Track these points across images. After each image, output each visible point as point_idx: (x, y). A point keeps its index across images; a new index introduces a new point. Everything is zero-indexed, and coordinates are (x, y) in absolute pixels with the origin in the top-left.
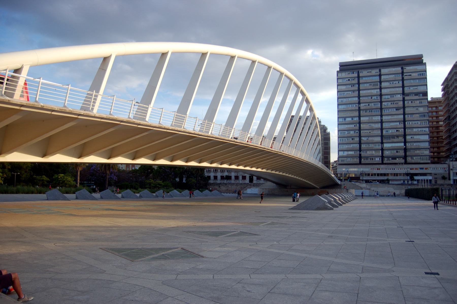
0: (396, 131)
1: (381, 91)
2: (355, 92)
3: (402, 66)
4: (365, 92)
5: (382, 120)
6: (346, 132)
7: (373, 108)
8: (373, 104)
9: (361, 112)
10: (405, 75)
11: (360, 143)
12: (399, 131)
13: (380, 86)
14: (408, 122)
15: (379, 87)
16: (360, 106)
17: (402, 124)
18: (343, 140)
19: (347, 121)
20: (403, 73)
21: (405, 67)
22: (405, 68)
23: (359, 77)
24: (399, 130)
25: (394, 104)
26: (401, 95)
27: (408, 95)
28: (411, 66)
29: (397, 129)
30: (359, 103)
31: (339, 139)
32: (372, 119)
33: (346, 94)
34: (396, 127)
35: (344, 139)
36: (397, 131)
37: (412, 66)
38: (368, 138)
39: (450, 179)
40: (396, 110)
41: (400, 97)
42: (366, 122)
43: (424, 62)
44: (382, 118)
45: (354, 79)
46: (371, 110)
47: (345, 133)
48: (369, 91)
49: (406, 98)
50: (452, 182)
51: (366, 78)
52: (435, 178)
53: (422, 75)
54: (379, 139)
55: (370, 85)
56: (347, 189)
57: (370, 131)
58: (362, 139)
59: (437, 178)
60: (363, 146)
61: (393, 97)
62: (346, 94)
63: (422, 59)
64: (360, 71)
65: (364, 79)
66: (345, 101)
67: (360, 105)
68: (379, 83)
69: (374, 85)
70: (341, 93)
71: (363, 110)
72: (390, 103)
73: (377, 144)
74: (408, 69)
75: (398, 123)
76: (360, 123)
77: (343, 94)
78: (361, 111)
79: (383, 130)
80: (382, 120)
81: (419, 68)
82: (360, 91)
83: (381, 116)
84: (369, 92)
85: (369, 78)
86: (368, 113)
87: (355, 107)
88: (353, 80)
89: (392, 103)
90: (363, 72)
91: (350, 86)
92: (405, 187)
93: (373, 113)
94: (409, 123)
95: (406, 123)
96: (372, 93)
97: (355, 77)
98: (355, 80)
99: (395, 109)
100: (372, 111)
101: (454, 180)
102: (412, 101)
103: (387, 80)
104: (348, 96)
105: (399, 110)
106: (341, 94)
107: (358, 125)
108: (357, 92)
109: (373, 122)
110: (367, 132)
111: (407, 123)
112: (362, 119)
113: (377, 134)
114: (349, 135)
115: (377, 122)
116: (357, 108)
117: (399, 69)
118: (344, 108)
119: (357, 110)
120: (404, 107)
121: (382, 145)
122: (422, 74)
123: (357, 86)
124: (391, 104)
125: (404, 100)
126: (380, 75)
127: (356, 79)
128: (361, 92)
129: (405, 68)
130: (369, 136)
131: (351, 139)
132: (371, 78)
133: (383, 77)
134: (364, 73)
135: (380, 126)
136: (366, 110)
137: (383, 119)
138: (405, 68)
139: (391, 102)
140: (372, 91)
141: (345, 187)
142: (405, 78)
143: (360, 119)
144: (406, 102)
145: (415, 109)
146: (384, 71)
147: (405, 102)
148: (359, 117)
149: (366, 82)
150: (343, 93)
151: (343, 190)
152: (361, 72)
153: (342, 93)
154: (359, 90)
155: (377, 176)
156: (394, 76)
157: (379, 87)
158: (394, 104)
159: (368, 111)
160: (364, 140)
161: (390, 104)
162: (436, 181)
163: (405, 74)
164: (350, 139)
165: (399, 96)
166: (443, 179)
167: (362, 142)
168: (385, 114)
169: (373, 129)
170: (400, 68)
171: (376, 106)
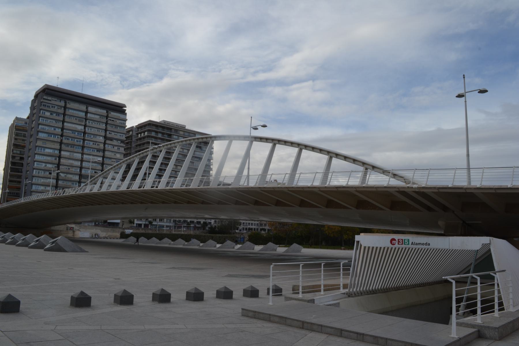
0: (94, 172)
1: (85, 128)
2: (59, 122)
3: (107, 110)
4: (69, 125)
5: (82, 158)
6: (44, 164)
7: (76, 144)
8: (76, 140)
9: (63, 146)
10: (109, 119)
11: (57, 179)
12: (98, 172)
13: (85, 123)
14: (106, 165)
15: (84, 124)
16: (62, 139)
17: (100, 166)
18: (39, 173)
19: (46, 152)
20: (107, 117)
21: (110, 111)
22: (110, 113)
23: (65, 108)
24: (97, 171)
25: (95, 144)
26: (103, 138)
27: (111, 139)
28: (115, 112)
29: (96, 171)
30: (62, 136)
31: (34, 170)
32: (73, 155)
33: (49, 121)
34: (95, 168)
35: (40, 171)
36: (95, 172)
37: (117, 113)
38: (66, 175)
39: (134, 224)
40: (97, 151)
41: (102, 139)
42: (67, 157)
43: (126, 112)
44: (82, 157)
45: (60, 108)
46: (73, 145)
47: (42, 165)
48: (74, 126)
49: (108, 142)
50: (135, 225)
51: (73, 111)
52: (123, 222)
53: (123, 124)
54: (77, 178)
55: (76, 119)
56: (74, 231)
57: (69, 167)
58: (60, 175)
59: (124, 222)
60: (60, 182)
61: (96, 137)
62: (49, 121)
63: (125, 108)
64: (67, 102)
65: (70, 111)
66: (48, 130)
67: (62, 138)
68: (84, 120)
69: (79, 121)
70: (44, 119)
71: (65, 144)
72: (92, 143)
73: (75, 183)
74: (113, 114)
75: (54, 158)
76: (60, 157)
77: (46, 120)
78: (63, 144)
79: (83, 169)
80: (82, 158)
81: (121, 116)
82: (65, 123)
83: (83, 154)
84: (74, 126)
85: (75, 112)
86: (69, 148)
87: (58, 139)
88: (59, 108)
89: (94, 143)
90: (71, 104)
91: (55, 114)
92: (111, 229)
93: (76, 150)
94: (107, 166)
95: (104, 165)
96: (77, 128)
97: (61, 107)
98: (61, 109)
99: (96, 150)
100: (73, 147)
101: (137, 224)
102: (114, 146)
103: (92, 119)
104: (51, 125)
105: (98, 152)
106: (44, 120)
107: (58, 159)
108: (61, 123)
109: (74, 158)
110: (66, 168)
111: (105, 166)
112: (63, 153)
113: (76, 172)
114: (46, 168)
115: (77, 160)
116: (59, 140)
117: (104, 112)
118: (45, 136)
119: (58, 142)
120: (104, 151)
121: (79, 184)
122: (123, 123)
123: (62, 117)
124: (93, 144)
125: (105, 144)
126: (87, 112)
127: (63, 109)
128: (65, 124)
129: (110, 112)
130: (67, 173)
131: (48, 173)
132: (77, 112)
133: (89, 115)
134: (71, 105)
135: (80, 164)
136: (68, 145)
137: (84, 158)
138: (110, 112)
139: (93, 143)
140: (77, 126)
141: (71, 229)
142: (109, 122)
143: (60, 152)
144: (107, 146)
145: (113, 154)
146: (91, 109)
147: (106, 145)
148: (60, 150)
149: (72, 114)
150: (46, 119)
151: (69, 231)
152: (68, 102)
153: (45, 119)
154: (63, 122)
155: (252, 228)
156: (99, 117)
157: (84, 124)
158: (95, 144)
159: (70, 146)
160: (62, 176)
161: (92, 143)
162: (124, 224)
163: (109, 118)
164: (47, 173)
165: (101, 138)
166: (130, 223)
167: (60, 178)
168: (86, 153)
169: (72, 166)
170: (105, 111)
171: (78, 143)
